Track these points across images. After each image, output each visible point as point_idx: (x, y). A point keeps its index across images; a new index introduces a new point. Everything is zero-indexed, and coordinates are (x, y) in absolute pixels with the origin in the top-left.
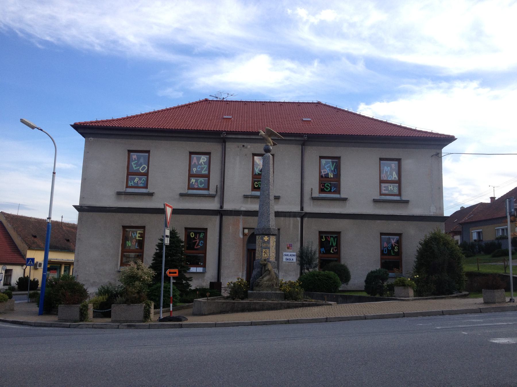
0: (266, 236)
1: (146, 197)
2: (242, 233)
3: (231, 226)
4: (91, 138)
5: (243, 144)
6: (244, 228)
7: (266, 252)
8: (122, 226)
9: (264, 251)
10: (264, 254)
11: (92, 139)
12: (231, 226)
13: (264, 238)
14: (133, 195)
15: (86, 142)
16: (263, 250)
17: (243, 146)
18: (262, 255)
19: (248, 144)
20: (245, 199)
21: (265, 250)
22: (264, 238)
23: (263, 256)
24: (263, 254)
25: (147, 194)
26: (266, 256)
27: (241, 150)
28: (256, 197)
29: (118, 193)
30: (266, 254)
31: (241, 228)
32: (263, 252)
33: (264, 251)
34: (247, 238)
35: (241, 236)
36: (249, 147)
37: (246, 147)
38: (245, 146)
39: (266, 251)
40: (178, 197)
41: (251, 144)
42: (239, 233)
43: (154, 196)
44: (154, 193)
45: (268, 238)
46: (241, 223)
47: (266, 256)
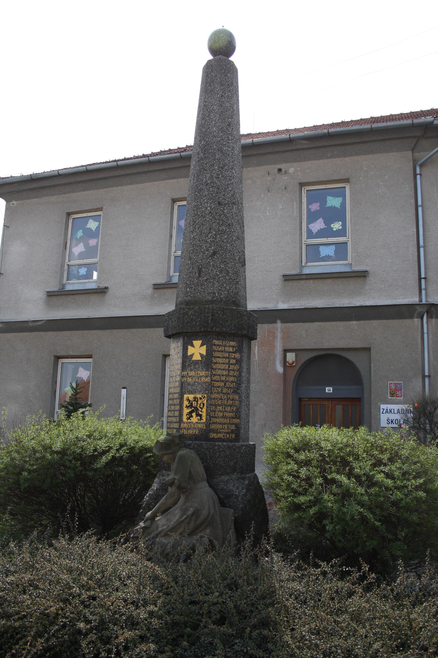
0: (207, 350)
1: (94, 298)
2: (282, 362)
3: (256, 348)
4: (13, 203)
5: (279, 166)
6: (286, 351)
7: (194, 404)
8: (55, 356)
9: (188, 400)
10: (190, 415)
11: (14, 202)
12: (256, 348)
13: (194, 358)
14: (73, 294)
15: (7, 209)
16: (186, 396)
17: (280, 170)
18: (181, 415)
19: (290, 164)
20: (286, 282)
21: (191, 397)
22: (194, 358)
23: (185, 419)
24: (186, 411)
25: (95, 291)
26: (194, 419)
27: (274, 179)
28: (309, 277)
29: (49, 294)
30: (194, 414)
31: (278, 349)
32: (186, 403)
33: (188, 400)
34: (293, 374)
35: (280, 369)
36: (291, 170)
37: (286, 172)
38: (283, 170)
39: (195, 399)
40: (150, 291)
41: (295, 164)
42: (274, 363)
43: (107, 294)
44: (106, 288)
45: (189, 354)
46: (279, 339)
47: (194, 419)
